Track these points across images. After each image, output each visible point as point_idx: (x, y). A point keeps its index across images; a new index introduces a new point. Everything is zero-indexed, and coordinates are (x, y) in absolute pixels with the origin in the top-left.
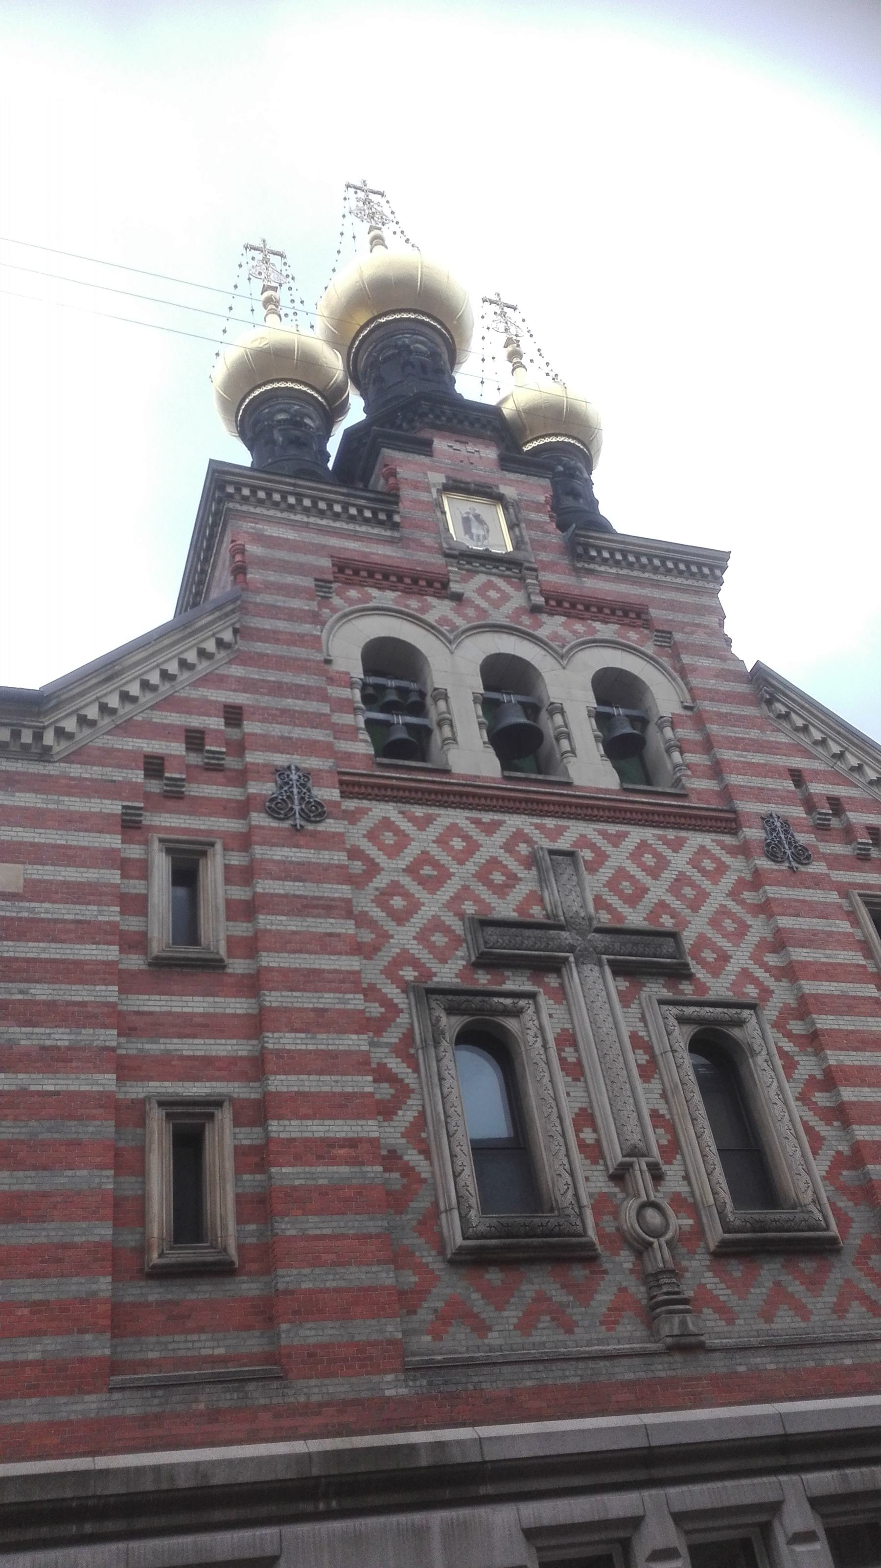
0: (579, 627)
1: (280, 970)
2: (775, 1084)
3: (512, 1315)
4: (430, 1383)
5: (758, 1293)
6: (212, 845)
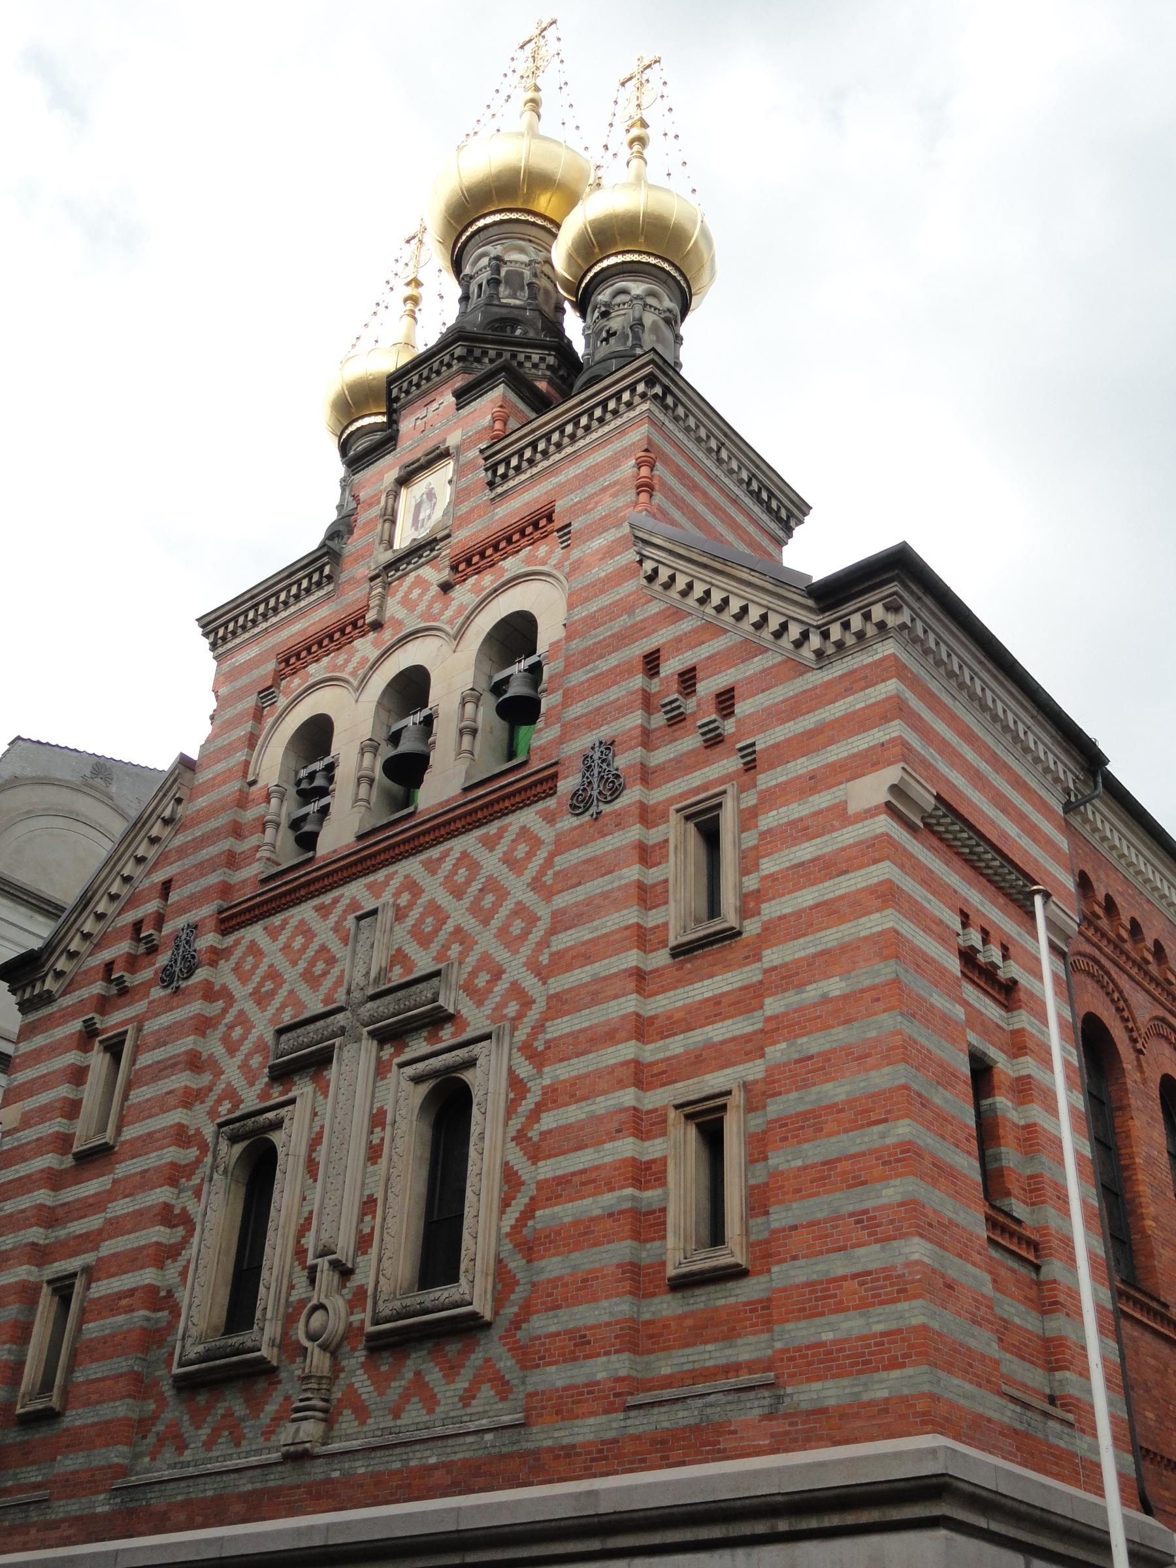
3: (205, 1432)
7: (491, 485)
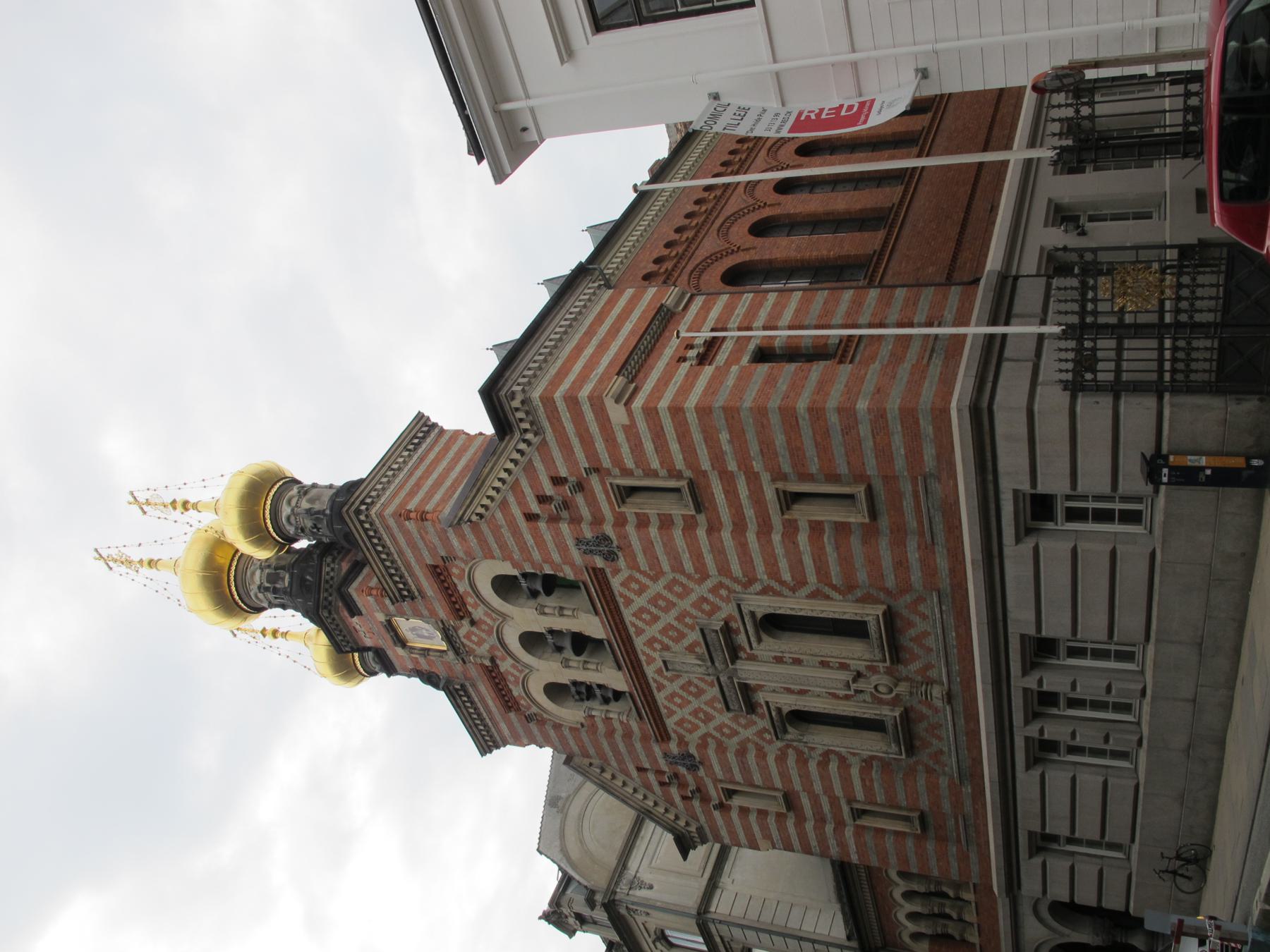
3: (935, 741)
7: (413, 598)
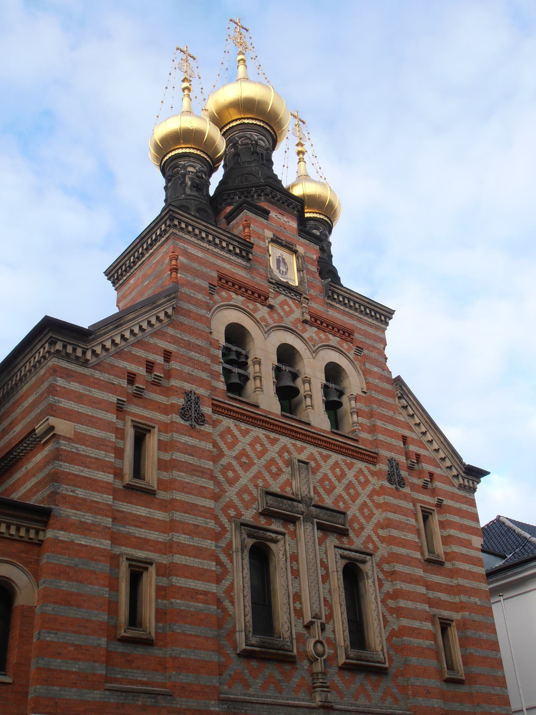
0: (322, 335)
1: (181, 501)
2: (374, 594)
3: (259, 682)
4: (228, 707)
5: (354, 687)
6: (154, 428)
